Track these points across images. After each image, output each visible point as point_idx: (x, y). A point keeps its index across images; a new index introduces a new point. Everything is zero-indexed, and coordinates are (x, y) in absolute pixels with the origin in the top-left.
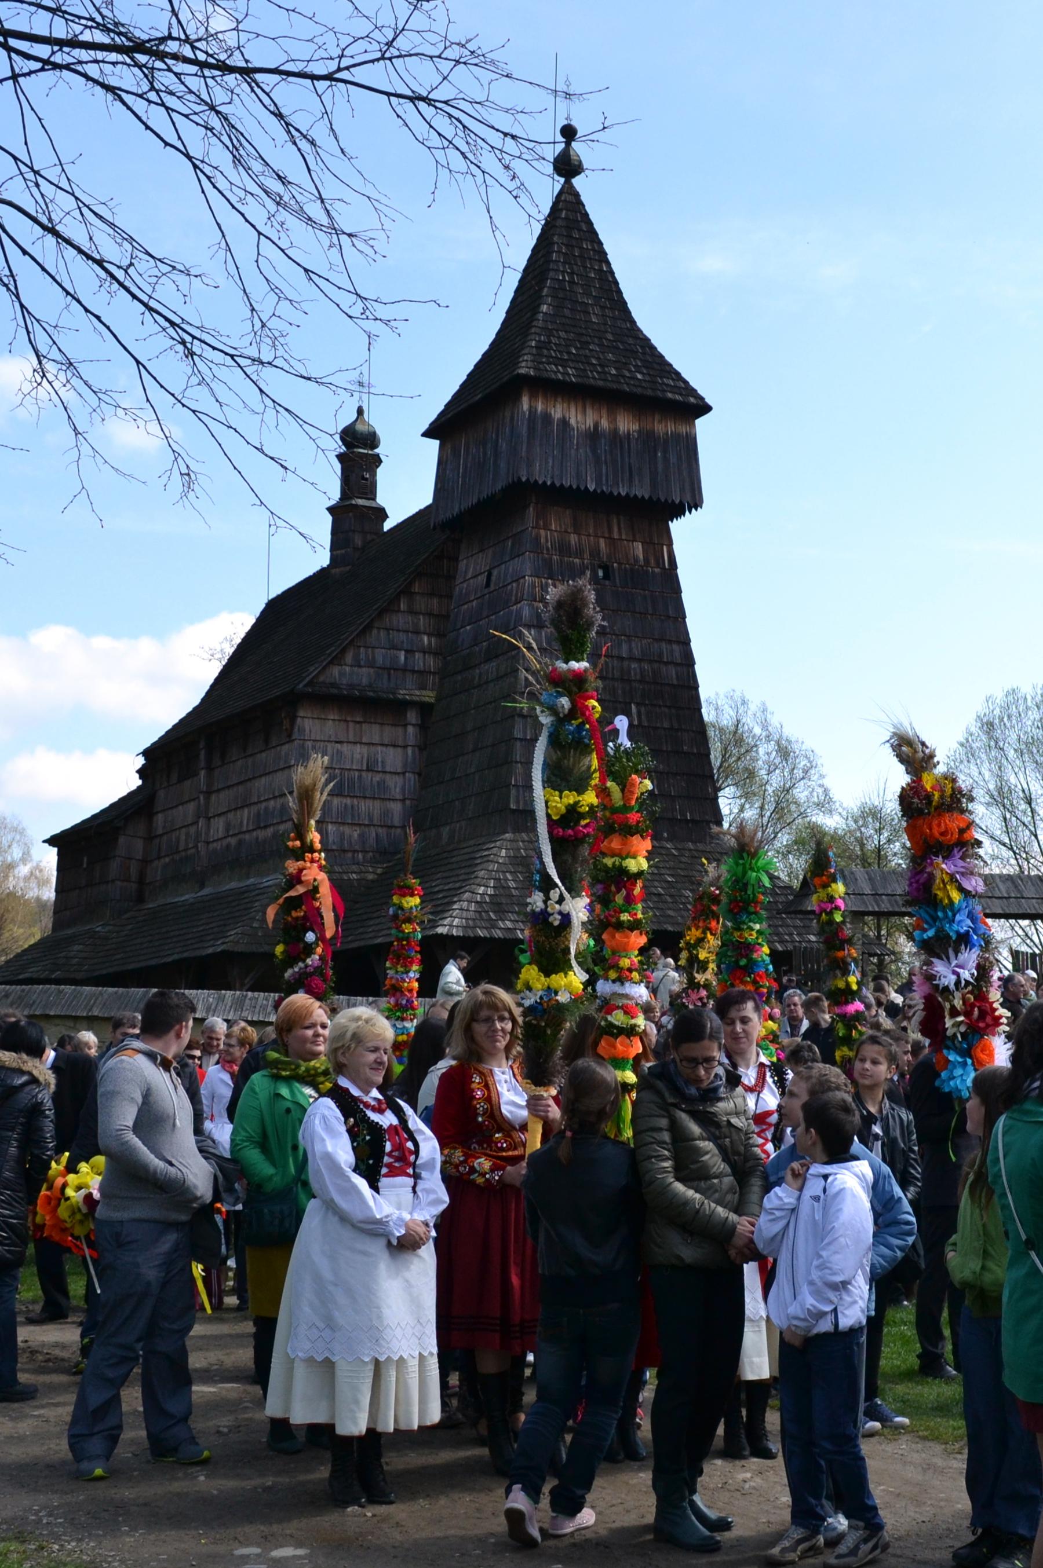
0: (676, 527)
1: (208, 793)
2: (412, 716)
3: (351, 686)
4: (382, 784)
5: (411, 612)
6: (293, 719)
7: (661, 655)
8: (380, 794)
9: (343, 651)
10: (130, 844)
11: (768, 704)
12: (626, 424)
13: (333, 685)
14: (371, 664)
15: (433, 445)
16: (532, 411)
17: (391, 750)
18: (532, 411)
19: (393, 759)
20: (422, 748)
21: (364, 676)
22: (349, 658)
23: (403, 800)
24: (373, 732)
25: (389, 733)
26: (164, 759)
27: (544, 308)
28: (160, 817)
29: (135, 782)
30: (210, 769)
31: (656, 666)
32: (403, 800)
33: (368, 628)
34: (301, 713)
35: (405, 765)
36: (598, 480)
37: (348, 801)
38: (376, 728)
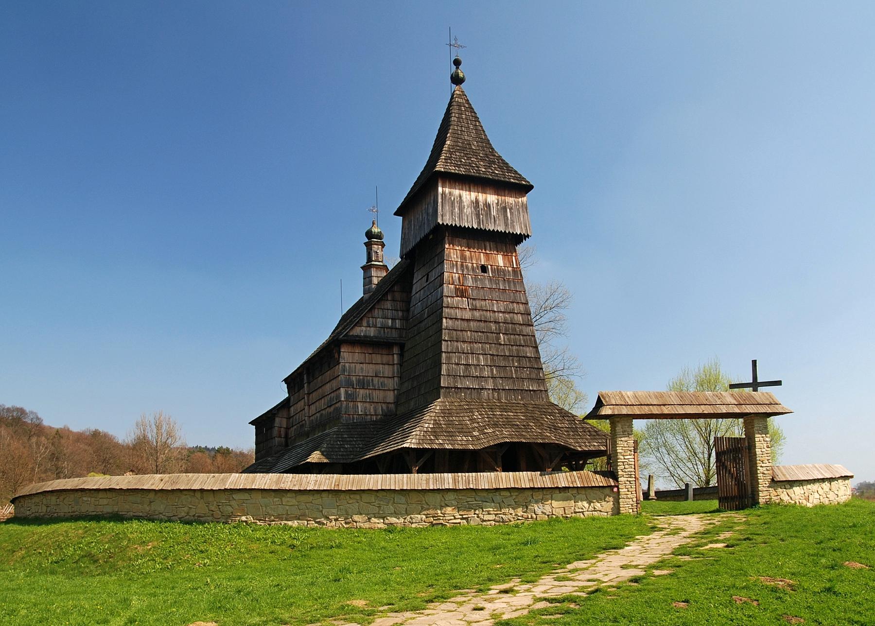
0: (519, 248)
1: (309, 394)
2: (396, 350)
3: (365, 336)
4: (383, 384)
5: (393, 300)
6: (339, 352)
7: (514, 309)
8: (382, 388)
9: (361, 319)
10: (280, 422)
11: (525, 243)
13: (357, 336)
14: (375, 326)
15: (400, 219)
16: (443, 193)
17: (387, 366)
18: (443, 193)
19: (387, 370)
20: (401, 365)
21: (372, 332)
22: (365, 323)
23: (394, 390)
24: (377, 358)
25: (385, 358)
26: (292, 381)
27: (448, 142)
28: (292, 409)
29: (282, 393)
30: (309, 383)
31: (511, 315)
32: (394, 390)
33: (373, 308)
34: (342, 350)
35: (394, 373)
36: (479, 223)
37: (367, 391)
38: (379, 356)
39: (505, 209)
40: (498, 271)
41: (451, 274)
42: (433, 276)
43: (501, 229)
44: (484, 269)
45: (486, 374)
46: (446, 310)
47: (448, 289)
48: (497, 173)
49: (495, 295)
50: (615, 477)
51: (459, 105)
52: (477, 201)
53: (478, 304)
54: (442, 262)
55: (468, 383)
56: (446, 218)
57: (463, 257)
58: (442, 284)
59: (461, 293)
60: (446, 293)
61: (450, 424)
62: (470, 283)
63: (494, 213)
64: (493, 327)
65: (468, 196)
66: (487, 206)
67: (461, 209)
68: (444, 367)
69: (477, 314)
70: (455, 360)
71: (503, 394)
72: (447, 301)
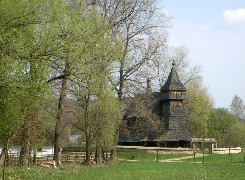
12: (179, 93)
39: (182, 95)
40: (180, 106)
41: (171, 108)
42: (168, 107)
43: (181, 99)
44: (177, 106)
45: (177, 126)
46: (170, 115)
47: (171, 111)
48: (180, 88)
49: (179, 111)
50: (193, 149)
51: (174, 71)
52: (176, 94)
53: (176, 113)
54: (170, 105)
55: (174, 129)
56: (171, 98)
57: (174, 104)
58: (169, 110)
59: (173, 111)
60: (170, 112)
61: (171, 136)
62: (175, 109)
63: (180, 96)
64: (178, 118)
65: (175, 93)
66: (178, 94)
67: (174, 96)
68: (170, 126)
69: (176, 116)
70: (172, 124)
71: (180, 130)
72: (171, 113)
